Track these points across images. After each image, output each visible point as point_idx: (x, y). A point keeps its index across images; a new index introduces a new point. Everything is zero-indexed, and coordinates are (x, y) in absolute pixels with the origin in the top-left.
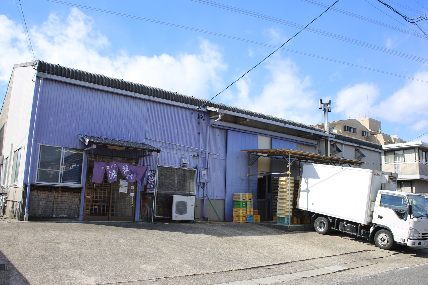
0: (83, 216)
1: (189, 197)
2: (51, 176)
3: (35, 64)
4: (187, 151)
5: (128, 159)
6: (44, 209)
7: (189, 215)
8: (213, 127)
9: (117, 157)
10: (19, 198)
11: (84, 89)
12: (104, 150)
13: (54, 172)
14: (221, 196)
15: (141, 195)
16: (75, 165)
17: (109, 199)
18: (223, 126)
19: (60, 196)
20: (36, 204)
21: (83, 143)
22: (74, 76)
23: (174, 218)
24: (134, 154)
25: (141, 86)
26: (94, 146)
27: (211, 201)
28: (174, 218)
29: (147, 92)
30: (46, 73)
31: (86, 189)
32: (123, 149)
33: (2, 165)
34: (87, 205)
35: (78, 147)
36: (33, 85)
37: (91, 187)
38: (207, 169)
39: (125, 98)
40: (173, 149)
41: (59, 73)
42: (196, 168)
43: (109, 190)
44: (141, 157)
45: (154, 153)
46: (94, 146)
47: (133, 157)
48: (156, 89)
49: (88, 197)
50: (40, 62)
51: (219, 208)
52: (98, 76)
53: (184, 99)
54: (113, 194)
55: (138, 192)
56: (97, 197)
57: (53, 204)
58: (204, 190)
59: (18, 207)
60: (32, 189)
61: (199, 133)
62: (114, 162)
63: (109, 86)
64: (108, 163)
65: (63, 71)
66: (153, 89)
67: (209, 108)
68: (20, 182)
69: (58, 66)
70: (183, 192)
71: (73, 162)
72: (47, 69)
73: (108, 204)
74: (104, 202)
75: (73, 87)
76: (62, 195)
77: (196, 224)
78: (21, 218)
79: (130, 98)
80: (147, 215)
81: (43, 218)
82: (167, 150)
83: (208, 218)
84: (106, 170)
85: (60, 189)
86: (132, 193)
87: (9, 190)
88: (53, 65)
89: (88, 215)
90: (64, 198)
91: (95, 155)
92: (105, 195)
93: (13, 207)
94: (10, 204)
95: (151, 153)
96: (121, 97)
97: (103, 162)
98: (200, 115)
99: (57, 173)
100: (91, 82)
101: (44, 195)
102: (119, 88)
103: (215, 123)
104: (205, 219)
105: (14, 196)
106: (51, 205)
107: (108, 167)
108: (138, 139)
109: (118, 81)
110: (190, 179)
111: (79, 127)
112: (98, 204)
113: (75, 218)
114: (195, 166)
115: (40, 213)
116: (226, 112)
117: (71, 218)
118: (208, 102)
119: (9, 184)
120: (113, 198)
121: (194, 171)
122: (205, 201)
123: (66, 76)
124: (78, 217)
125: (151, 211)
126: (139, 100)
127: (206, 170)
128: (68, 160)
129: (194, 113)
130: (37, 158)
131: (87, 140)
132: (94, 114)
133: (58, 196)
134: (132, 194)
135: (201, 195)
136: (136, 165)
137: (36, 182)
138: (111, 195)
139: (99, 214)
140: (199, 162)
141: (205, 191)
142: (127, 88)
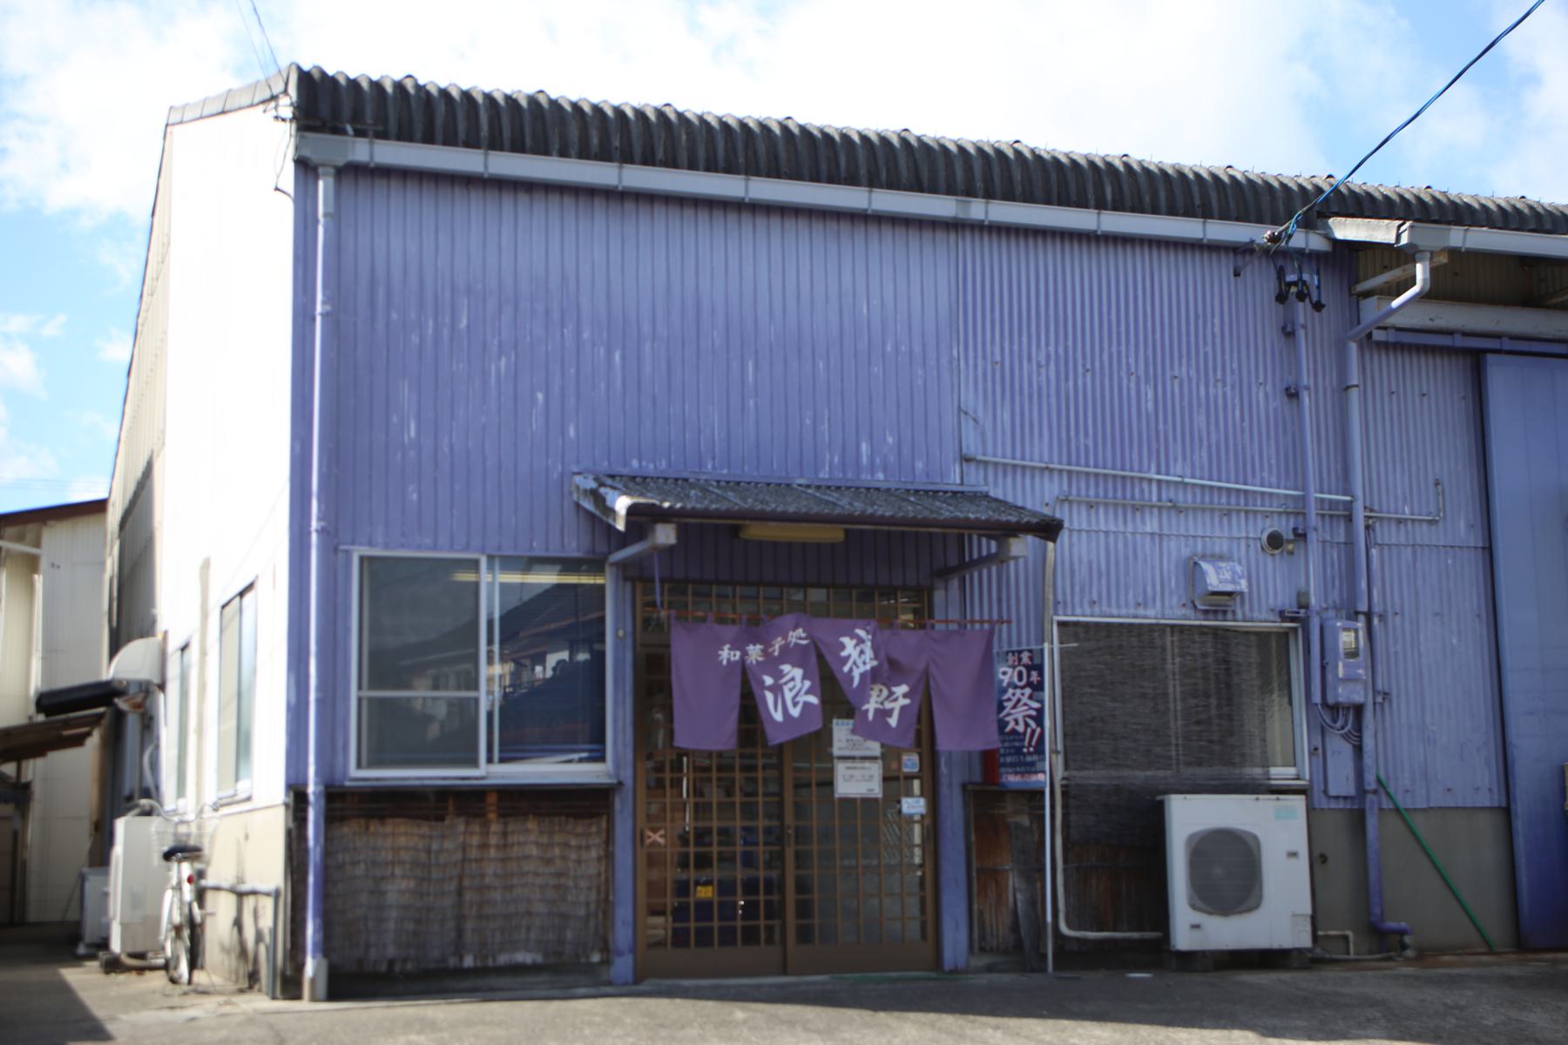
0: (634, 950)
1: (1267, 801)
2: (434, 731)
3: (278, 88)
4: (1228, 513)
5: (867, 595)
6: (410, 926)
7: (1282, 913)
8: (1385, 346)
9: (804, 585)
10: (270, 871)
11: (568, 201)
12: (726, 555)
13: (451, 703)
14: (1475, 783)
15: (966, 804)
16: (565, 655)
17: (780, 840)
18: (1450, 333)
19: (493, 840)
20: (364, 898)
21: (599, 518)
22: (507, 133)
23: (1183, 939)
24: (904, 558)
25: (904, 141)
26: (665, 535)
27: (1418, 822)
28: (1183, 939)
29: (942, 175)
30: (343, 132)
31: (642, 789)
32: (835, 534)
33: (162, 687)
34: (651, 885)
35: (574, 547)
36: (285, 210)
37: (667, 775)
38: (1369, 616)
39: (818, 226)
40: (1135, 509)
41: (419, 127)
42: (1298, 616)
43: (774, 788)
44: (944, 573)
45: (1022, 546)
46: (665, 535)
47: (898, 581)
48: (999, 152)
49: (658, 838)
50: (305, 78)
51: (1475, 858)
52: (640, 114)
53: (1178, 191)
54: (800, 810)
55: (944, 790)
56: (709, 831)
57: (460, 892)
58: (1359, 750)
59: (266, 922)
60: (338, 815)
61: (1292, 394)
62: (788, 619)
63: (711, 167)
64: (755, 629)
65: (441, 109)
66: (980, 150)
67: (1348, 230)
68: (268, 780)
69: (409, 84)
70: (1225, 771)
71: (552, 639)
72: (347, 111)
73: (774, 874)
74: (749, 860)
75: (507, 200)
76: (505, 834)
77: (1331, 974)
78: (290, 986)
79: (845, 227)
80: (1015, 928)
81: (408, 977)
82: (1105, 521)
83: (1402, 932)
84: (743, 668)
85: (492, 799)
86: (909, 794)
87: (209, 829)
88: (377, 86)
89: (660, 944)
90: (515, 852)
91: (676, 585)
92: (754, 816)
93: (238, 923)
94: (221, 911)
95: (1003, 546)
96: (790, 223)
97: (721, 620)
98: (1291, 278)
99: (466, 710)
100: (604, 155)
101: (402, 841)
102: (774, 172)
103: (1391, 321)
104: (1385, 941)
105: (240, 862)
106: (449, 901)
107: (755, 652)
108: (919, 465)
109: (764, 127)
110: (1265, 688)
111: (563, 432)
112: (715, 873)
113: (590, 969)
114: (1285, 600)
115: (387, 947)
116: (1458, 237)
117: (566, 969)
118: (1336, 190)
119: (210, 797)
120: (801, 835)
121: (1284, 636)
122: (1372, 822)
123: (462, 135)
124: (606, 962)
125: (1036, 903)
126: (900, 231)
127: (1361, 625)
128: (524, 626)
129: (1247, 273)
130: (348, 630)
131: (622, 504)
132: (647, 347)
133: (484, 846)
134: (914, 805)
135: (1341, 781)
136: (923, 627)
137: (357, 774)
138: (789, 819)
139: (728, 937)
140: (1311, 574)
141: (1368, 760)
142: (824, 166)
